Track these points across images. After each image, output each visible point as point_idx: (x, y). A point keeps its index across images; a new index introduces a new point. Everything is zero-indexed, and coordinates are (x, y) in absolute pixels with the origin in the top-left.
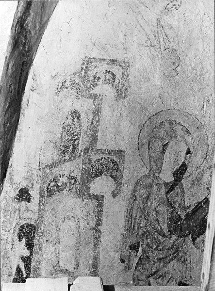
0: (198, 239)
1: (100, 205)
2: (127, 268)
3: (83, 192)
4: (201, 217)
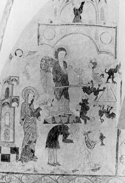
0: (38, 118)
1: (14, 109)
2: (22, 125)
3: (10, 106)
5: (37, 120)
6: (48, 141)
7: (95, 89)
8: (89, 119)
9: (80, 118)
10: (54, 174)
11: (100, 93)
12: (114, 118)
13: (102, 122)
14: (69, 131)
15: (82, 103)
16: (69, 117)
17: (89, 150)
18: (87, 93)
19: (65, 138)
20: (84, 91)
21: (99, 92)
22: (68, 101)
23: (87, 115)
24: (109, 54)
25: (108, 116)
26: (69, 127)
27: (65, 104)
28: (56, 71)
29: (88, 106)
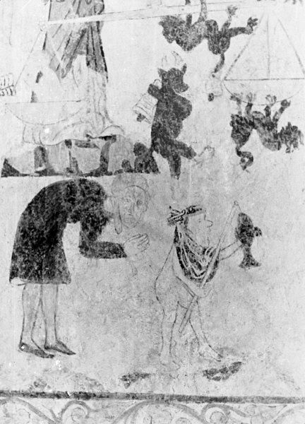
6: (18, 251)
7: (211, 26)
8: (189, 153)
9: (154, 153)
10: (47, 390)
11: (236, 42)
12: (295, 146)
13: (245, 168)
14: (108, 206)
15: (160, 86)
16: (107, 146)
17: (193, 285)
18: (178, 42)
19: (92, 236)
20: (166, 33)
21: (228, 41)
22: (99, 77)
23: (180, 138)
25: (269, 141)
26: (107, 189)
27: (91, 93)
29: (184, 99)
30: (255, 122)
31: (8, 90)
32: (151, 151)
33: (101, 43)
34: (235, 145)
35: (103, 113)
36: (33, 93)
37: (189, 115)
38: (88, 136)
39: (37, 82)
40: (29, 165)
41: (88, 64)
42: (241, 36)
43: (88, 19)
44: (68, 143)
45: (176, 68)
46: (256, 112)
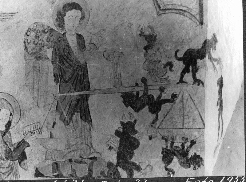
0: (22, 163)
4: (22, 150)
5: (20, 169)
9: (118, 168)
11: (165, 107)
15: (121, 130)
16: (92, 163)
18: (131, 107)
20: (124, 102)
22: (88, 126)
23: (133, 160)
24: (186, 14)
25: (184, 163)
27: (83, 134)
28: (61, 56)
29: (135, 138)
30: (176, 152)
31: (37, 131)
32: (117, 166)
33: (88, 107)
34: (164, 165)
35: (90, 145)
36: (51, 133)
37: (138, 147)
38: (81, 157)
39: (53, 127)
40: (49, 172)
41: (81, 118)
42: (168, 104)
43: (82, 93)
44: (70, 161)
45: (131, 121)
46: (176, 147)
